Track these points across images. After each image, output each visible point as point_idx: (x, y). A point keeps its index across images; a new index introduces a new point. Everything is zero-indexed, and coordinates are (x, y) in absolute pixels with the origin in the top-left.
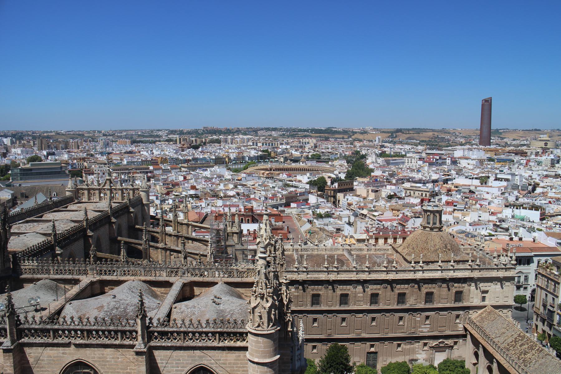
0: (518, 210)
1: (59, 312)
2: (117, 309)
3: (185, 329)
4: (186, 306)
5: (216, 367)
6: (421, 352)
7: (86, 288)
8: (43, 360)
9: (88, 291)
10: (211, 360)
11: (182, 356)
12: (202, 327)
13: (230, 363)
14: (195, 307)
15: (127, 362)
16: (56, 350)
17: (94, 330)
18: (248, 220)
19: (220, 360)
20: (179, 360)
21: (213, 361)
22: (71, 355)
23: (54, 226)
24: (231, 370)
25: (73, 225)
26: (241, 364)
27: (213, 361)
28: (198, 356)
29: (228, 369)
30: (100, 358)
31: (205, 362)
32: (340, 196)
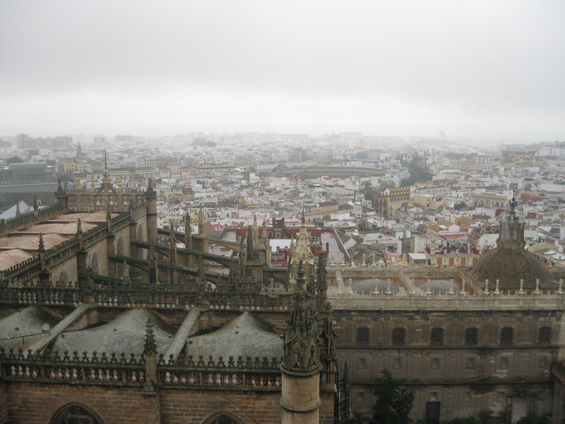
1: (51, 345)
2: (120, 343)
3: (204, 369)
4: (204, 341)
5: (241, 416)
6: (495, 403)
7: (81, 316)
8: (32, 403)
9: (84, 322)
10: (235, 408)
11: (199, 402)
12: (224, 367)
14: (214, 341)
15: (133, 408)
17: (92, 368)
19: (246, 407)
20: (196, 406)
21: (238, 409)
23: (41, 242)
24: (259, 420)
25: (64, 239)
27: (238, 409)
28: (220, 403)
31: (230, 410)
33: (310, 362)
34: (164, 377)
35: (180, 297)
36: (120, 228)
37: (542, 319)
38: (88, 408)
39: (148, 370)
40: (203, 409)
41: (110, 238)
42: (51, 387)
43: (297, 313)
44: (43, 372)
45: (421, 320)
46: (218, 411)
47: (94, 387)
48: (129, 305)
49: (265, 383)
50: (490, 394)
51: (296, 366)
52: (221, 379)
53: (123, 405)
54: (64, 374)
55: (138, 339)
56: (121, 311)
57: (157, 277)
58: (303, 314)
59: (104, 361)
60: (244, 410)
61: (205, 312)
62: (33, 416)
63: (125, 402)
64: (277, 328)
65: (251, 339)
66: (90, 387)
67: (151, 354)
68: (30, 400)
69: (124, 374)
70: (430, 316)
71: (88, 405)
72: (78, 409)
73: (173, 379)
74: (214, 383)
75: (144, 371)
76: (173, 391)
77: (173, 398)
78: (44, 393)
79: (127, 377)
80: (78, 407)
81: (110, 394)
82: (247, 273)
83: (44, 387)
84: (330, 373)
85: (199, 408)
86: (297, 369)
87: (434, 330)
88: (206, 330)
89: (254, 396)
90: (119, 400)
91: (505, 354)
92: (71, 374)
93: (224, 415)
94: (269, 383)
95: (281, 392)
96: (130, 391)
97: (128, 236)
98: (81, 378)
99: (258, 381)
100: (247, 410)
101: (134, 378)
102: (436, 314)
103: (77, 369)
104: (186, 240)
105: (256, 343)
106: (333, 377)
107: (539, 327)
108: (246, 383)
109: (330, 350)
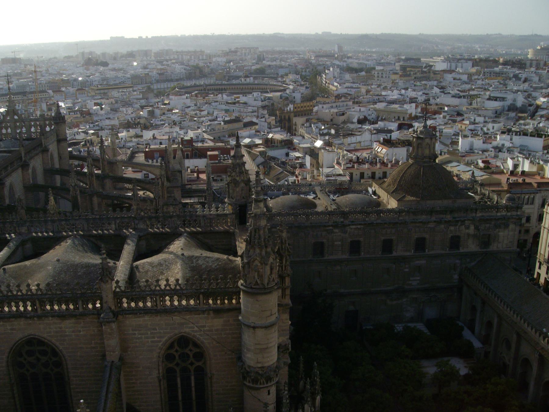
0: (518, 137)
5: (199, 335)
18: (187, 155)
19: (204, 326)
21: (196, 329)
22: (21, 330)
27: (196, 329)
29: (216, 337)
31: (187, 330)
32: (299, 121)
34: (122, 303)
37: (452, 228)
38: (45, 339)
39: (104, 296)
43: (255, 232)
45: (339, 234)
46: (177, 332)
47: (50, 318)
49: (222, 301)
50: (405, 300)
51: (257, 283)
52: (178, 301)
53: (81, 333)
56: (56, 241)
57: (80, 203)
58: (262, 232)
60: (202, 329)
67: (107, 281)
69: (80, 303)
71: (45, 335)
73: (130, 304)
76: (130, 316)
77: (132, 321)
80: (35, 338)
81: (68, 325)
84: (285, 289)
85: (158, 330)
86: (257, 287)
87: (352, 243)
89: (212, 314)
91: (417, 262)
92: (25, 306)
93: (182, 336)
94: (226, 301)
95: (240, 309)
98: (36, 310)
99: (215, 300)
100: (205, 329)
101: (90, 306)
102: (354, 227)
103: (30, 302)
104: (101, 164)
105: (203, 264)
106: (288, 292)
107: (450, 236)
109: (285, 266)
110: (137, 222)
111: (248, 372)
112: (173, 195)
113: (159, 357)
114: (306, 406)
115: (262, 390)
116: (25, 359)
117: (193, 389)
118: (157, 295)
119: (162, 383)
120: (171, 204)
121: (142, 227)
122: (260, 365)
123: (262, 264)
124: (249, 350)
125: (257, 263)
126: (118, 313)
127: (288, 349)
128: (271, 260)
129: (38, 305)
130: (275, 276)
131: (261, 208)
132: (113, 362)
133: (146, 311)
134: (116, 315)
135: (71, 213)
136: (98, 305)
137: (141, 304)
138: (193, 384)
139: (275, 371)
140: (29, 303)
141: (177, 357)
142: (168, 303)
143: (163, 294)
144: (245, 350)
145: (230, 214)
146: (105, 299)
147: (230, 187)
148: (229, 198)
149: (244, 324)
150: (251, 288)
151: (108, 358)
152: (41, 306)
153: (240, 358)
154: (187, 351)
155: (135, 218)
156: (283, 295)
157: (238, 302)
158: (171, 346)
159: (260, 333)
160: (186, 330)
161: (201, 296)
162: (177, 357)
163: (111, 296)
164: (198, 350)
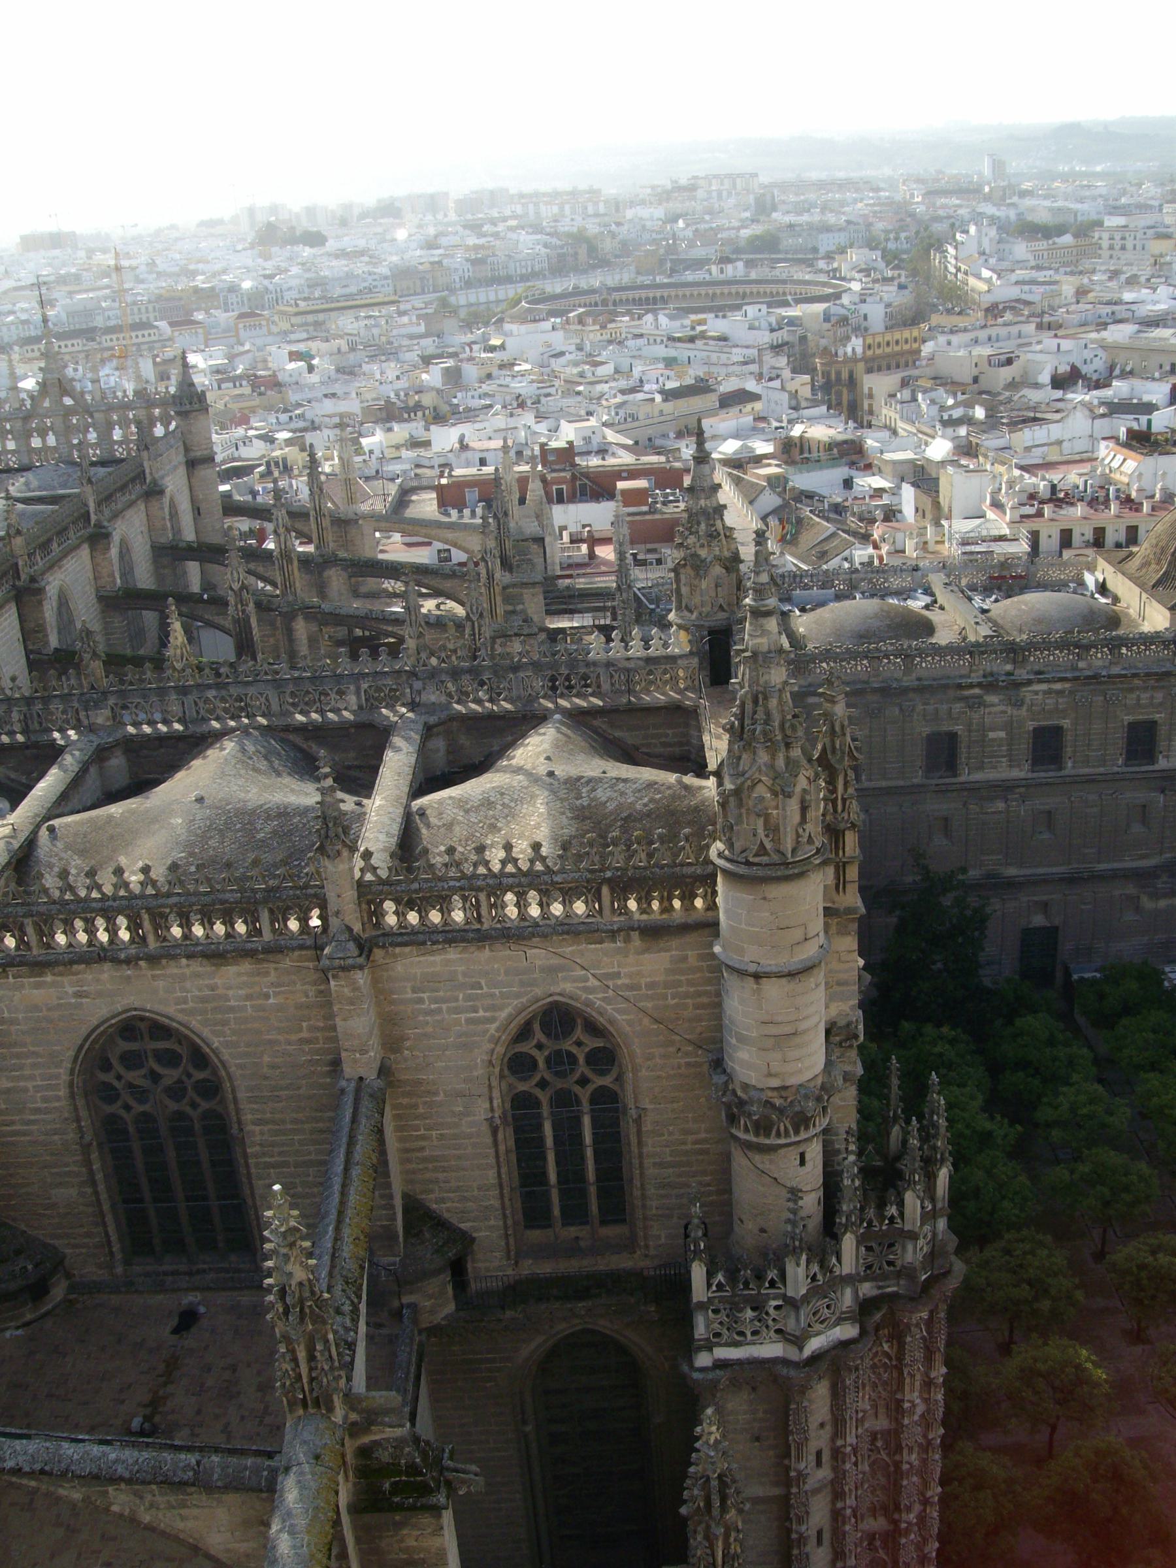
8: (13, 1022)
10: (587, 980)
13: (651, 985)
15: (299, 1007)
16: (53, 984)
19: (618, 975)
21: (593, 982)
22: (105, 996)
26: (690, 983)
27: (593, 982)
28: (543, 970)
29: (649, 1005)
30: (204, 1000)
31: (568, 987)
33: (798, 836)
34: (380, 914)
35: (358, 689)
36: (120, 506)
39: (331, 896)
40: (497, 991)
41: (98, 538)
42: (61, 974)
43: (755, 702)
44: (31, 936)
46: (538, 991)
47: (184, 961)
48: (215, 724)
49: (666, 904)
52: (541, 904)
53: (271, 1001)
54: (91, 931)
55: (269, 818)
56: (192, 744)
58: (773, 703)
59: (122, 893)
61: (436, 726)
62: (18, 1056)
63: (276, 994)
64: (647, 754)
65: (593, 790)
66: (172, 963)
67: (339, 853)
68: (6, 1015)
69: (265, 916)
70: (1027, 693)
71: (171, 1010)
72: (143, 1026)
73: (404, 915)
74: (523, 916)
75: (323, 907)
76: (407, 949)
77: (410, 965)
78: (42, 991)
79: (272, 924)
80: (142, 1019)
81: (233, 978)
82: (510, 608)
83: (40, 975)
84: (845, 864)
88: (443, 774)
89: (636, 941)
90: (257, 989)
92: (112, 931)
93: (556, 1002)
94: (677, 904)
95: (716, 924)
96: (287, 963)
97: (145, 529)
98: (144, 939)
100: (619, 982)
101: (293, 925)
103: (128, 917)
104: (314, 526)
105: (610, 799)
106: (853, 873)
108: (613, 910)
109: (844, 800)
110: (418, 685)
111: (741, 1103)
112: (519, 607)
113: (490, 1061)
114: (909, 1196)
115: (782, 1151)
116: (119, 1078)
117: (589, 1153)
118: (479, 889)
119: (500, 1136)
120: (516, 635)
121: (433, 698)
122: (775, 1083)
123: (775, 794)
124: (742, 1039)
125: (761, 791)
126: (371, 944)
127: (856, 1037)
128: (802, 783)
129: (147, 924)
130: (814, 828)
131: (769, 632)
132: (361, 1079)
133: (450, 936)
134: (365, 947)
135: (232, 665)
136: (315, 922)
137: (435, 917)
138: (588, 1138)
139: (819, 1099)
140: (122, 921)
141: (541, 1064)
142: (512, 912)
143: (497, 885)
144: (734, 1041)
145: (681, 657)
146: (332, 907)
147: (683, 577)
148: (679, 608)
149: (728, 966)
150: (748, 863)
151: (348, 1070)
152: (156, 927)
153: (718, 1064)
154: (568, 1045)
155: (413, 674)
156: (840, 884)
157: (712, 906)
158: (524, 1033)
159: (773, 989)
160: (566, 987)
161: (605, 891)
162: (541, 1064)
163: (350, 894)
164: (599, 1043)
